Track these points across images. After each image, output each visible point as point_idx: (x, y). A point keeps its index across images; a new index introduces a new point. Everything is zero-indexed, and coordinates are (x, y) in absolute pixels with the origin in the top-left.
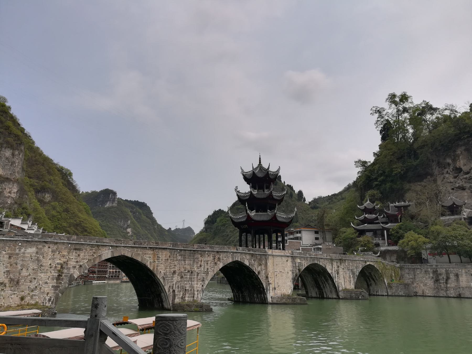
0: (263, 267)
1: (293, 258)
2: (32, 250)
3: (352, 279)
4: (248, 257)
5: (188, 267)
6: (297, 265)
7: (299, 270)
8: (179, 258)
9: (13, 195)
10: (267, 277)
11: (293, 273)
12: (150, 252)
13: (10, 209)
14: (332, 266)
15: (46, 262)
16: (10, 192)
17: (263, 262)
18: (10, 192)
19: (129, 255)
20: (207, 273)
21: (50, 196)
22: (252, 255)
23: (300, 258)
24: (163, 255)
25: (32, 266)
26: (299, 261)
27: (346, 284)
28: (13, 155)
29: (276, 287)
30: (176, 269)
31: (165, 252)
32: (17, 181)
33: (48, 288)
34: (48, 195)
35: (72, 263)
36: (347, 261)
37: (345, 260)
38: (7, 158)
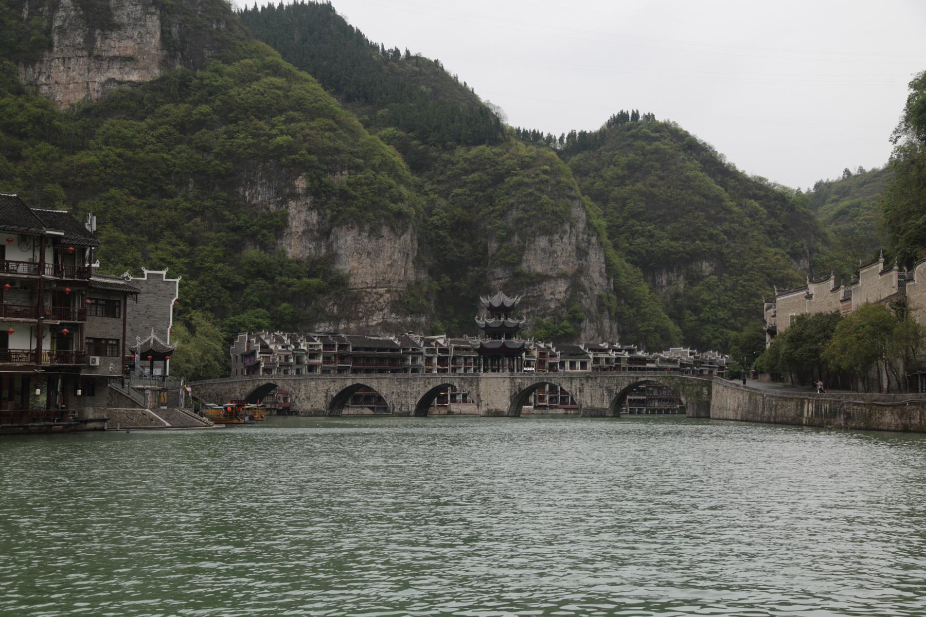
0: (474, 387)
1: (512, 379)
2: (313, 383)
3: (606, 398)
4: (458, 380)
5: (404, 389)
6: (517, 384)
7: (520, 389)
8: (396, 383)
9: (558, 296)
10: (478, 396)
11: (511, 392)
12: (376, 380)
13: (553, 315)
14: (571, 383)
15: (320, 389)
16: (552, 294)
17: (475, 383)
18: (552, 294)
19: (362, 383)
20: (419, 393)
21: (712, 265)
22: (462, 379)
23: (521, 378)
24: (384, 382)
25: (314, 391)
26: (520, 381)
27: (594, 403)
28: (551, 242)
29: (489, 403)
30: (395, 391)
31: (385, 380)
32: (563, 276)
33: (322, 402)
34: (707, 264)
35: (332, 389)
36: (599, 379)
37: (596, 378)
38: (543, 250)
